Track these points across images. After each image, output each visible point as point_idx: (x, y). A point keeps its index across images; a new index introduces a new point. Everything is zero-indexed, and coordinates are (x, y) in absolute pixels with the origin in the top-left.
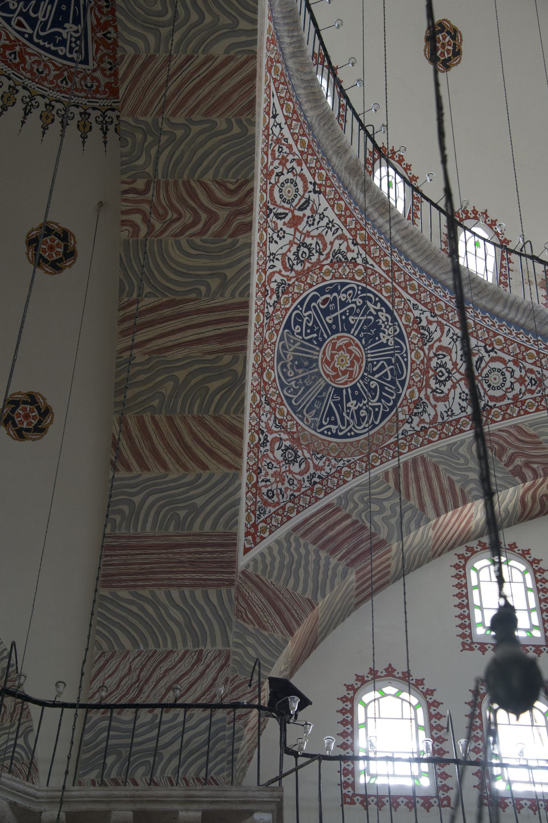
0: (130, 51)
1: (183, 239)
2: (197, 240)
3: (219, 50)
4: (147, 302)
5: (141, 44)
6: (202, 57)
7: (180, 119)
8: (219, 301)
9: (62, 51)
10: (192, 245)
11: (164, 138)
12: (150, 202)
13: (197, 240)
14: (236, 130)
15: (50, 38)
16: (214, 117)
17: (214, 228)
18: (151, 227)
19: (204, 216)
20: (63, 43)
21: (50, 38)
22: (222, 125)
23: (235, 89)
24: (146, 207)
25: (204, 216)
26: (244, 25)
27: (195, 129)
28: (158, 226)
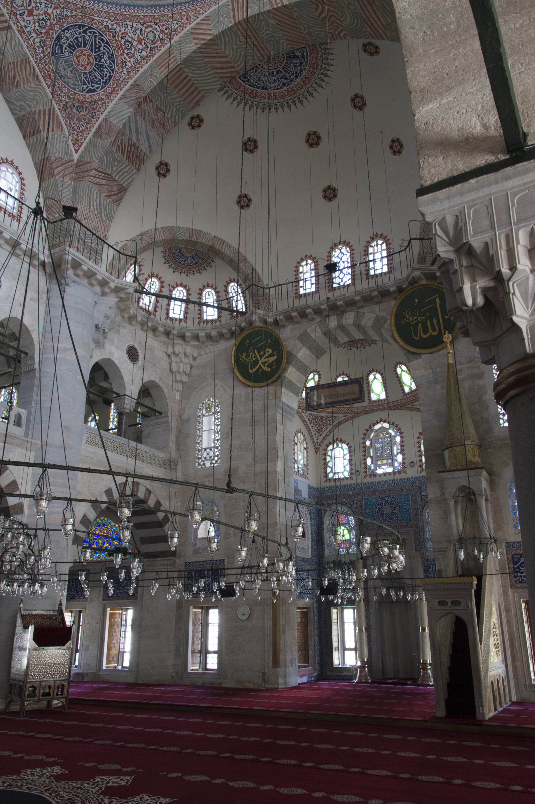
0: (289, 46)
1: (342, 19)
2: (340, 14)
3: (273, 22)
4: (369, 30)
5: (285, 44)
6: (278, 26)
7: (302, 27)
8: (357, 5)
9: (305, 54)
10: (342, 16)
11: (311, 30)
12: (334, 31)
13: (340, 14)
14: (295, 9)
15: (304, 58)
16: (295, 17)
17: (333, 9)
18: (342, 30)
19: (330, 13)
20: (303, 54)
21: (304, 58)
22: (296, 14)
23: (283, 14)
24: (336, 32)
25: (330, 13)
26: (261, 17)
27: (302, 22)
28: (341, 28)
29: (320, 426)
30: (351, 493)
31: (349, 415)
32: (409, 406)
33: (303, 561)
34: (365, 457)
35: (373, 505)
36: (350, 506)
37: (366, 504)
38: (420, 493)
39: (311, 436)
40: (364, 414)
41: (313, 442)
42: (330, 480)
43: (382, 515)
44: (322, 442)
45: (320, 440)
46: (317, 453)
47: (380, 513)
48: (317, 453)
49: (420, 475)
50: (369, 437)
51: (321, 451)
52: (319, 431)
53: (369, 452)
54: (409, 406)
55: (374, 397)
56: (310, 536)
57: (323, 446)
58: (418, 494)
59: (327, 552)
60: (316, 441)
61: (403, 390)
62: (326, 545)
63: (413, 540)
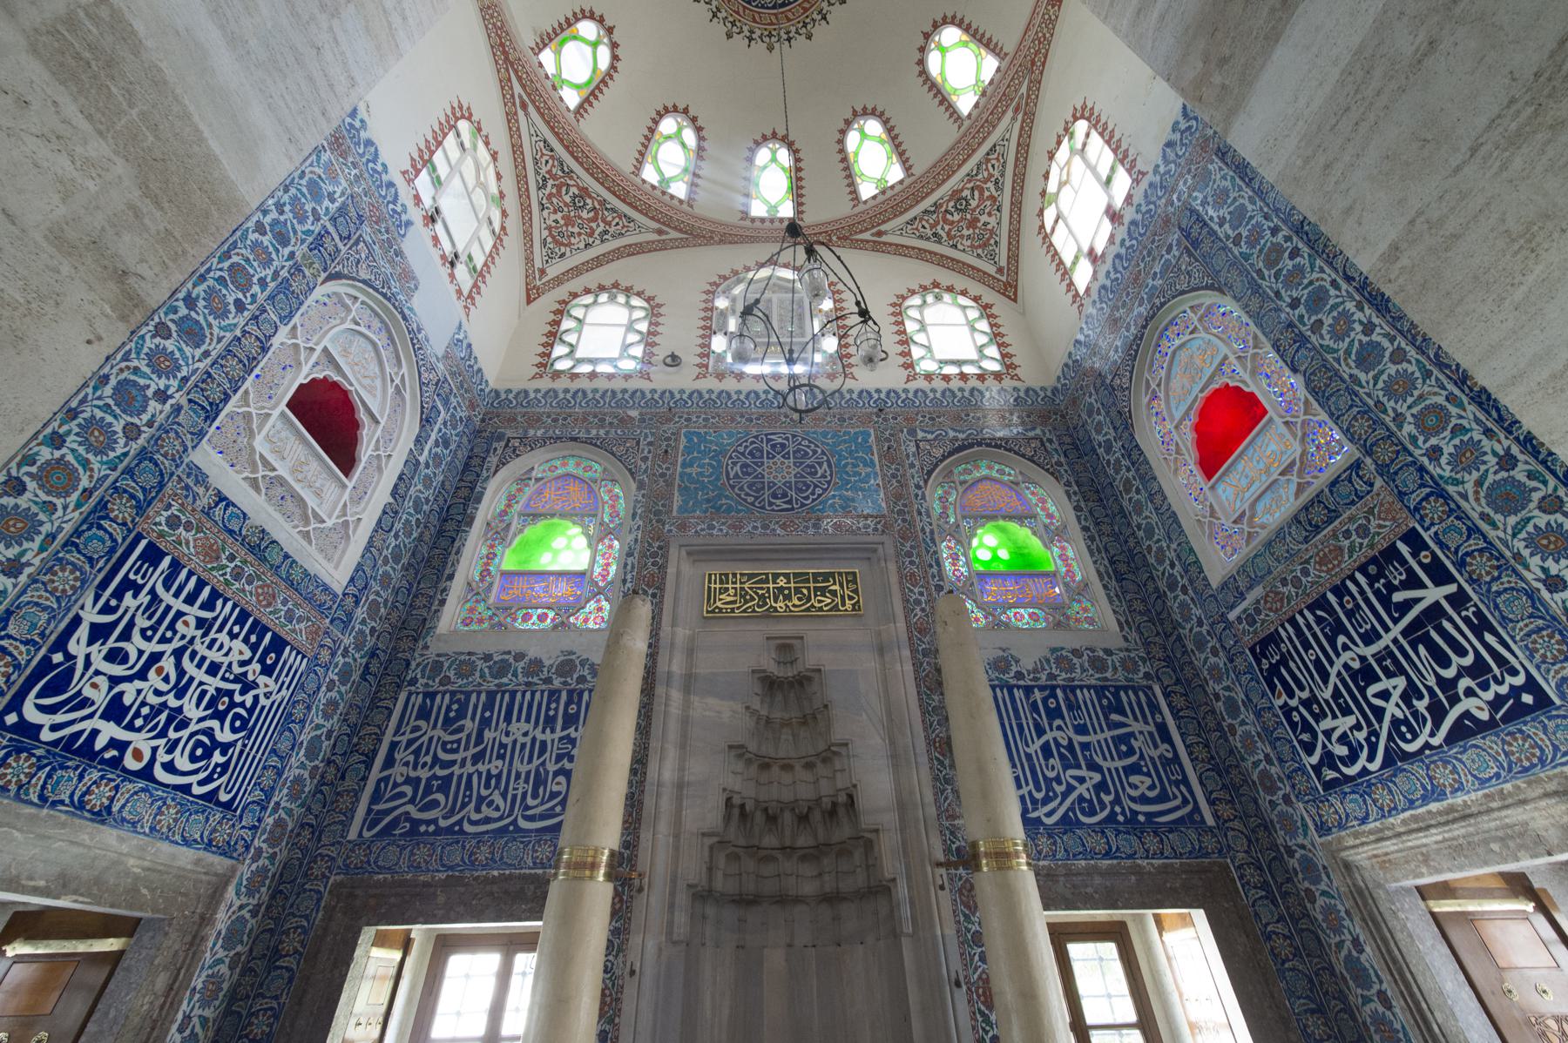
29: (569, 221)
30: (634, 413)
31: (674, 234)
32: (867, 236)
33: (253, 549)
34: (708, 332)
35: (723, 453)
36: (619, 450)
37: (688, 450)
38: (912, 432)
39: (528, 235)
40: (721, 242)
41: (529, 260)
42: (557, 374)
43: (757, 487)
44: (559, 281)
45: (553, 271)
46: (529, 302)
47: (766, 448)
48: (529, 302)
49: (908, 386)
50: (729, 289)
51: (548, 302)
52: (558, 241)
53: (725, 323)
54: (867, 236)
55: (758, 210)
56: (381, 496)
57: (561, 292)
58: (904, 436)
59: (451, 616)
60: (538, 264)
61: (854, 193)
62: (457, 587)
63: (894, 579)
